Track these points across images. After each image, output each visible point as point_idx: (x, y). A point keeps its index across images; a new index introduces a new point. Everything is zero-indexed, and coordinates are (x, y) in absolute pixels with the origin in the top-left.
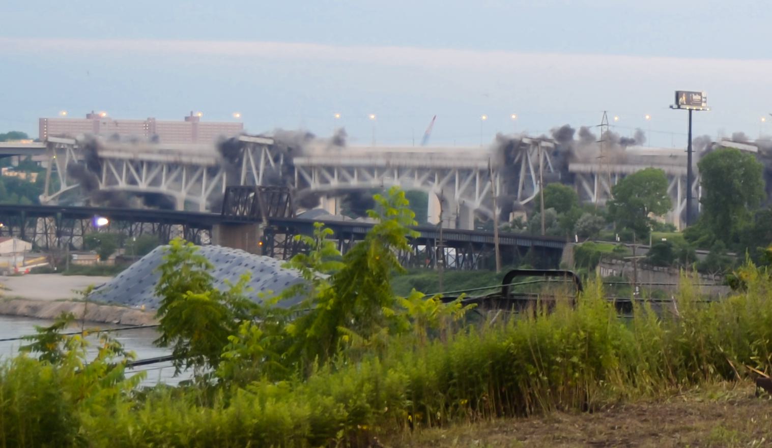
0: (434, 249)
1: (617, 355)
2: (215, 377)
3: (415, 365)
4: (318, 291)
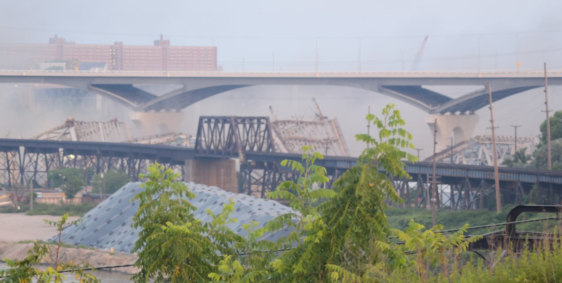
0: (427, 186)
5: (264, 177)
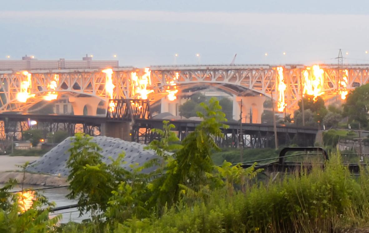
0: (237, 136)
1: (350, 198)
2: (104, 217)
3: (227, 207)
4: (167, 163)
5: (146, 132)
